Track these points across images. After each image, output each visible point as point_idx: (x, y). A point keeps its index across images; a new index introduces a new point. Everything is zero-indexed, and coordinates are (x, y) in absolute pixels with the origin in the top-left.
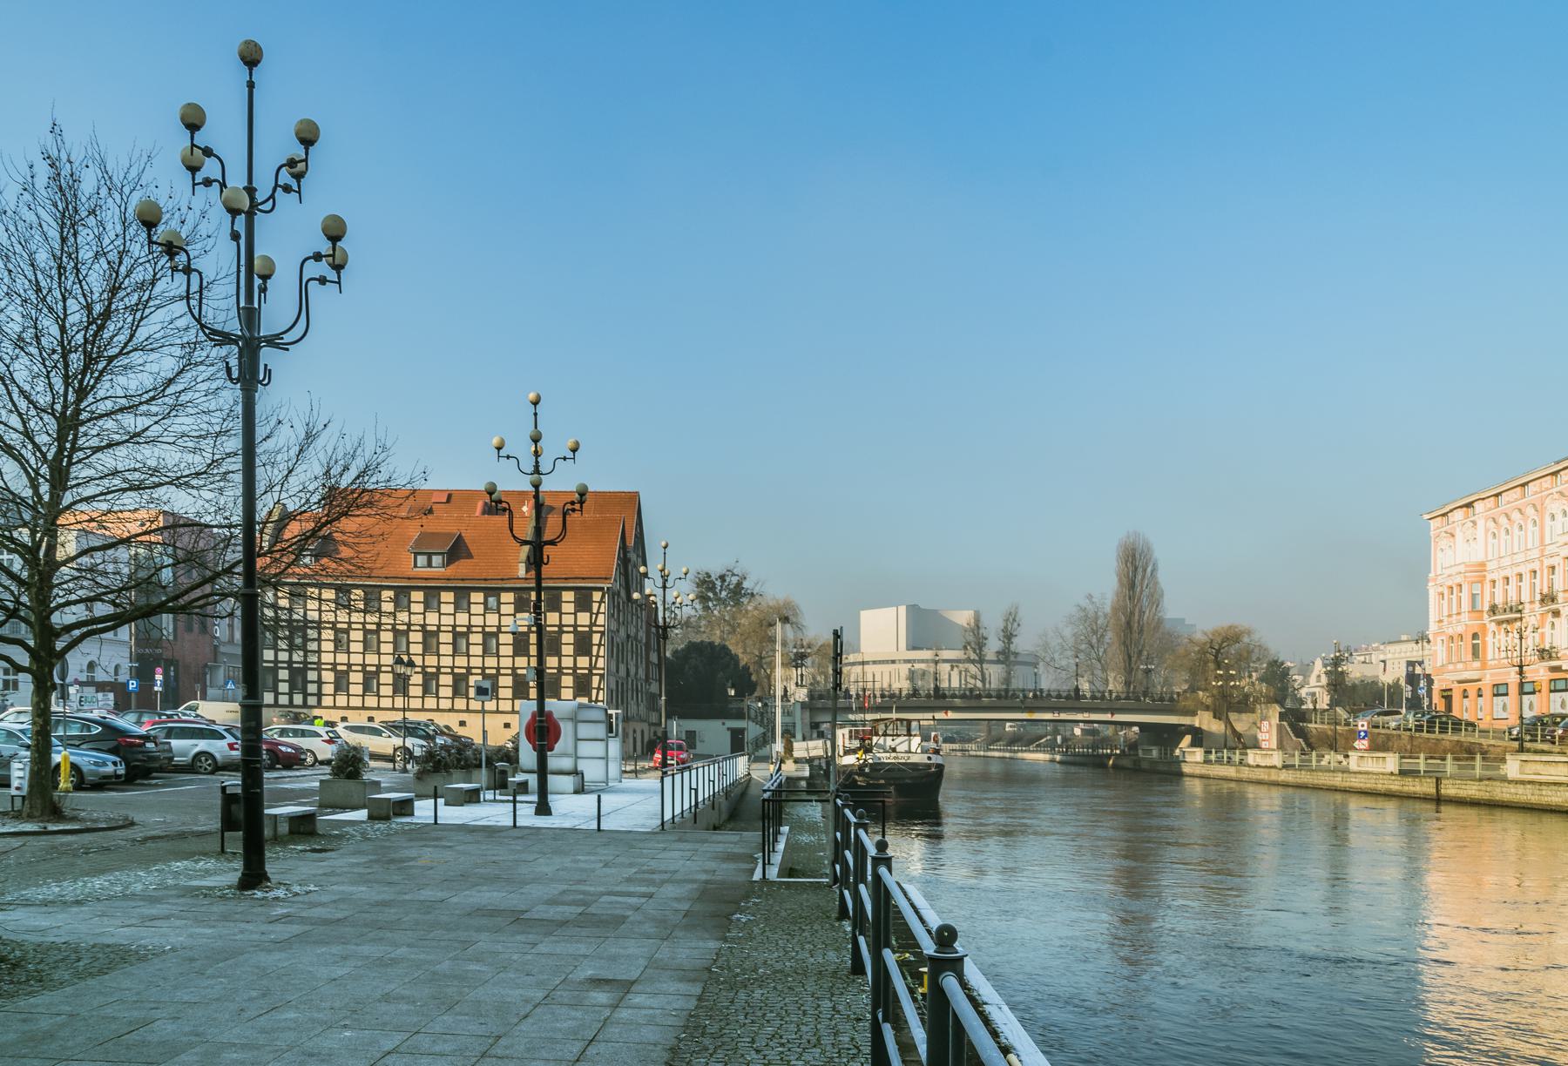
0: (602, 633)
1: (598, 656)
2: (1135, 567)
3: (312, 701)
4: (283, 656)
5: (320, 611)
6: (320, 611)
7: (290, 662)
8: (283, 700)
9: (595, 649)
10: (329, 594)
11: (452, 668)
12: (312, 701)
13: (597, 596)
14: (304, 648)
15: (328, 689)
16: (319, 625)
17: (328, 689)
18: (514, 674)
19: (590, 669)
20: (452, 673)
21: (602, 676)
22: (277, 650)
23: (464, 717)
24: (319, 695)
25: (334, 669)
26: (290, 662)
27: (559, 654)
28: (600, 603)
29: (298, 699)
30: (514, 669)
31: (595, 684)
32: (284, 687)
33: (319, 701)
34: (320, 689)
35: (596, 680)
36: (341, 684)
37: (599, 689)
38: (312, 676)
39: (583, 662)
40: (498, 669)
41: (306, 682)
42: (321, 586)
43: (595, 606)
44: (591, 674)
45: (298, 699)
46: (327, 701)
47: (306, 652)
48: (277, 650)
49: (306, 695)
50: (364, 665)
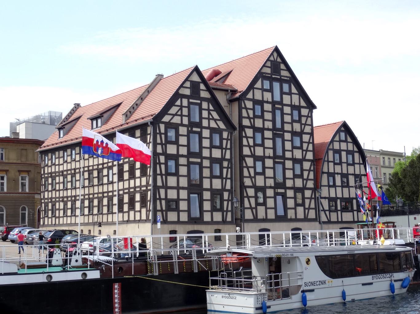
1: (150, 176)
18: (119, 195)
31: (149, 199)
36: (65, 210)
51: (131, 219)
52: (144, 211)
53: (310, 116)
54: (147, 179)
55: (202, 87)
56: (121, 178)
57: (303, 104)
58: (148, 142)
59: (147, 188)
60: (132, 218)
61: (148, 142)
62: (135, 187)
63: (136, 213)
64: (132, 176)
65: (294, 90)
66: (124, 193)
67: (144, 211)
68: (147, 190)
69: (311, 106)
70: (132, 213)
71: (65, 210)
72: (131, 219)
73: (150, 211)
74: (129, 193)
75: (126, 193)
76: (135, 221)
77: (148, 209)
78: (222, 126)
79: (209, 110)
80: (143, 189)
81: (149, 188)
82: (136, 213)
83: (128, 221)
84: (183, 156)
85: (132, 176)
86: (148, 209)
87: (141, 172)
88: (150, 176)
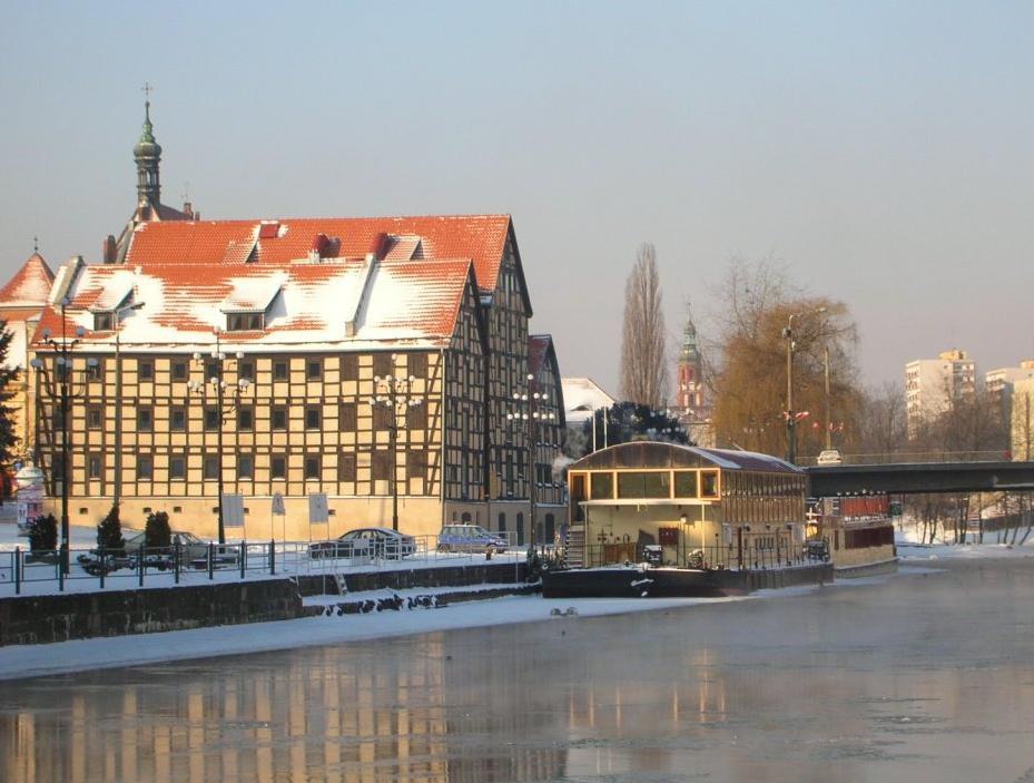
0: (439, 402)
1: (434, 429)
2: (649, 255)
9: (431, 420)
11: (270, 447)
13: (433, 359)
15: (129, 475)
17: (129, 475)
19: (426, 444)
20: (270, 453)
21: (438, 452)
25: (136, 452)
26: (86, 446)
27: (394, 430)
28: (436, 366)
35: (431, 457)
36: (145, 469)
37: (435, 467)
40: (322, 446)
43: (431, 371)
44: (426, 450)
47: (105, 433)
50: (170, 447)
53: (526, 330)
54: (426, 434)
55: (471, 293)
57: (523, 310)
58: (431, 375)
59: (426, 446)
61: (431, 375)
65: (518, 289)
69: (529, 312)
71: (145, 469)
73: (433, 481)
77: (429, 479)
78: (481, 353)
79: (474, 327)
84: (460, 399)
86: (429, 479)
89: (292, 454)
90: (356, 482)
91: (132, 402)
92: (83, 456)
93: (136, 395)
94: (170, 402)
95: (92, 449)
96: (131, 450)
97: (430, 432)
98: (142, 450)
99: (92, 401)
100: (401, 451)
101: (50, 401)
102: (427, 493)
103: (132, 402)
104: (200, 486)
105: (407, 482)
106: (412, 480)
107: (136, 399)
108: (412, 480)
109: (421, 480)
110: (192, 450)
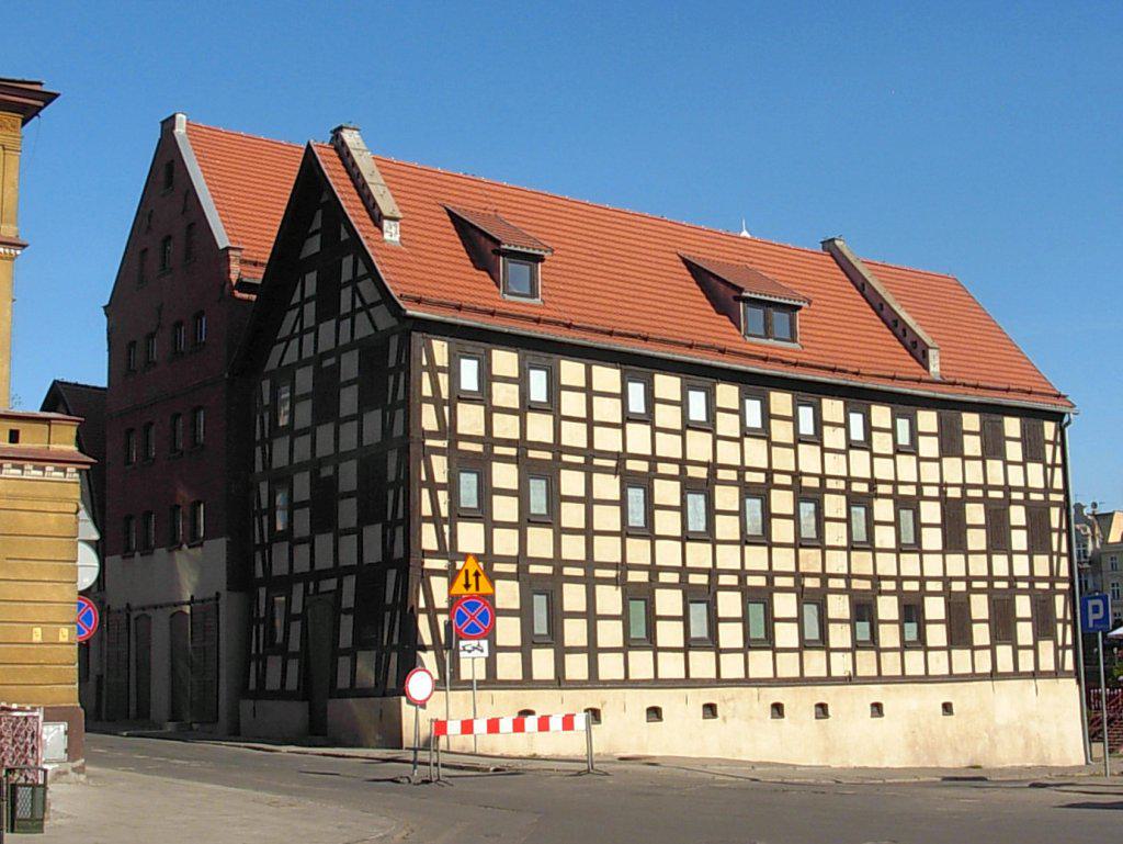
3: (576, 667)
4: (506, 542)
5: (590, 422)
6: (590, 422)
7: (522, 559)
8: (509, 667)
10: (607, 377)
12: (576, 667)
14: (551, 520)
15: (610, 634)
16: (589, 459)
18: (947, 593)
20: (848, 590)
22: (491, 526)
23: (876, 692)
24: (592, 650)
26: (522, 559)
27: (1010, 553)
29: (543, 663)
30: (946, 580)
32: (509, 631)
33: (593, 667)
34: (592, 633)
35: (1060, 600)
38: (574, 597)
39: (1042, 565)
41: (556, 615)
42: (591, 355)
45: (543, 663)
46: (610, 667)
48: (491, 526)
49: (561, 652)
51: (1000, 669)
52: (1046, 647)
56: (954, 539)
59: (1052, 585)
60: (1005, 664)
62: (1012, 579)
63: (1021, 652)
64: (998, 540)
66: (970, 590)
67: (1046, 647)
68: (1053, 592)
70: (1004, 652)
72: (1000, 669)
74: (990, 591)
75: (979, 591)
76: (1016, 674)
77: (1060, 643)
80: (1038, 585)
81: (1059, 586)
82: (1021, 652)
83: (994, 675)
85: (998, 540)
86: (1060, 643)
87: (1030, 539)
88: (1060, 554)
89: (881, 593)
90: (948, 649)
91: (612, 463)
92: (516, 585)
93: (619, 448)
94: (683, 471)
95: (534, 569)
96: (611, 574)
97: (1055, 558)
98: (633, 576)
99: (532, 454)
100: (934, 594)
101: (443, 444)
102: (1058, 673)
103: (612, 463)
104: (741, 656)
105: (1035, 648)
106: (1042, 644)
107: (621, 457)
108: (1042, 644)
109: (1051, 643)
110: (724, 580)
